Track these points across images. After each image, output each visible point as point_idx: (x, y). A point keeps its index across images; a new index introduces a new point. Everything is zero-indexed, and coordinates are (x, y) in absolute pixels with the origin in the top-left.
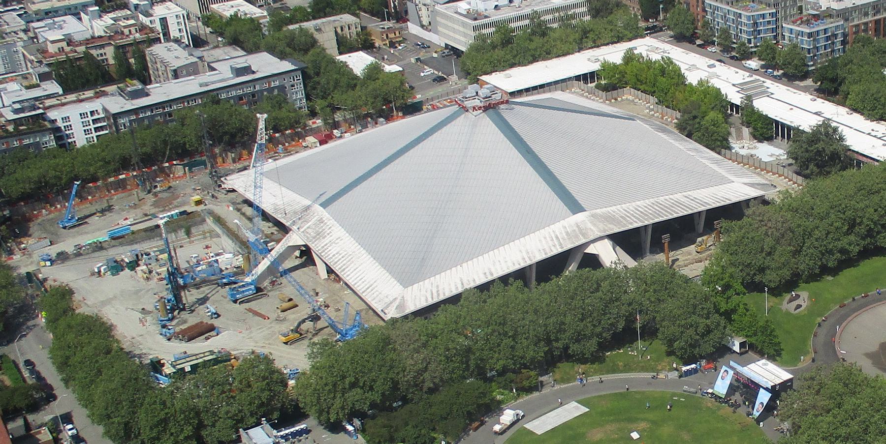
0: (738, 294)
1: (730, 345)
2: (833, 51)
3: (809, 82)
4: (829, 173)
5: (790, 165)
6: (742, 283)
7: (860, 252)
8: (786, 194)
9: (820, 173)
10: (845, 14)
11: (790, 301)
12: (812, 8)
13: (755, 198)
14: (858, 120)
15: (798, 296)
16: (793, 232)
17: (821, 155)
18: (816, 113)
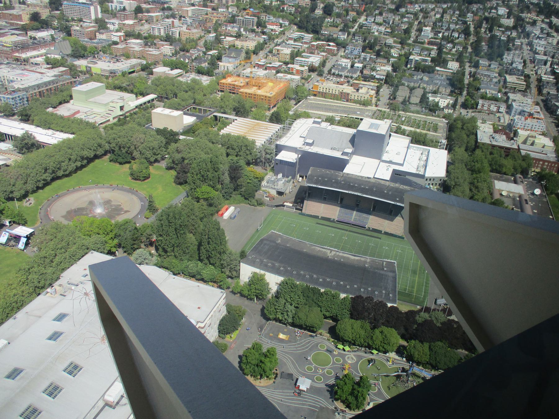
0: (4, 203)
1: (4, 223)
2: (23, 104)
3: (16, 117)
4: (32, 151)
5: (15, 150)
6: (4, 199)
7: (51, 180)
8: (16, 161)
9: (28, 152)
10: (26, 90)
11: (27, 202)
12: (11, 88)
13: (2, 165)
14: (40, 130)
15: (29, 200)
16: (22, 176)
17: (27, 145)
18: (22, 129)
